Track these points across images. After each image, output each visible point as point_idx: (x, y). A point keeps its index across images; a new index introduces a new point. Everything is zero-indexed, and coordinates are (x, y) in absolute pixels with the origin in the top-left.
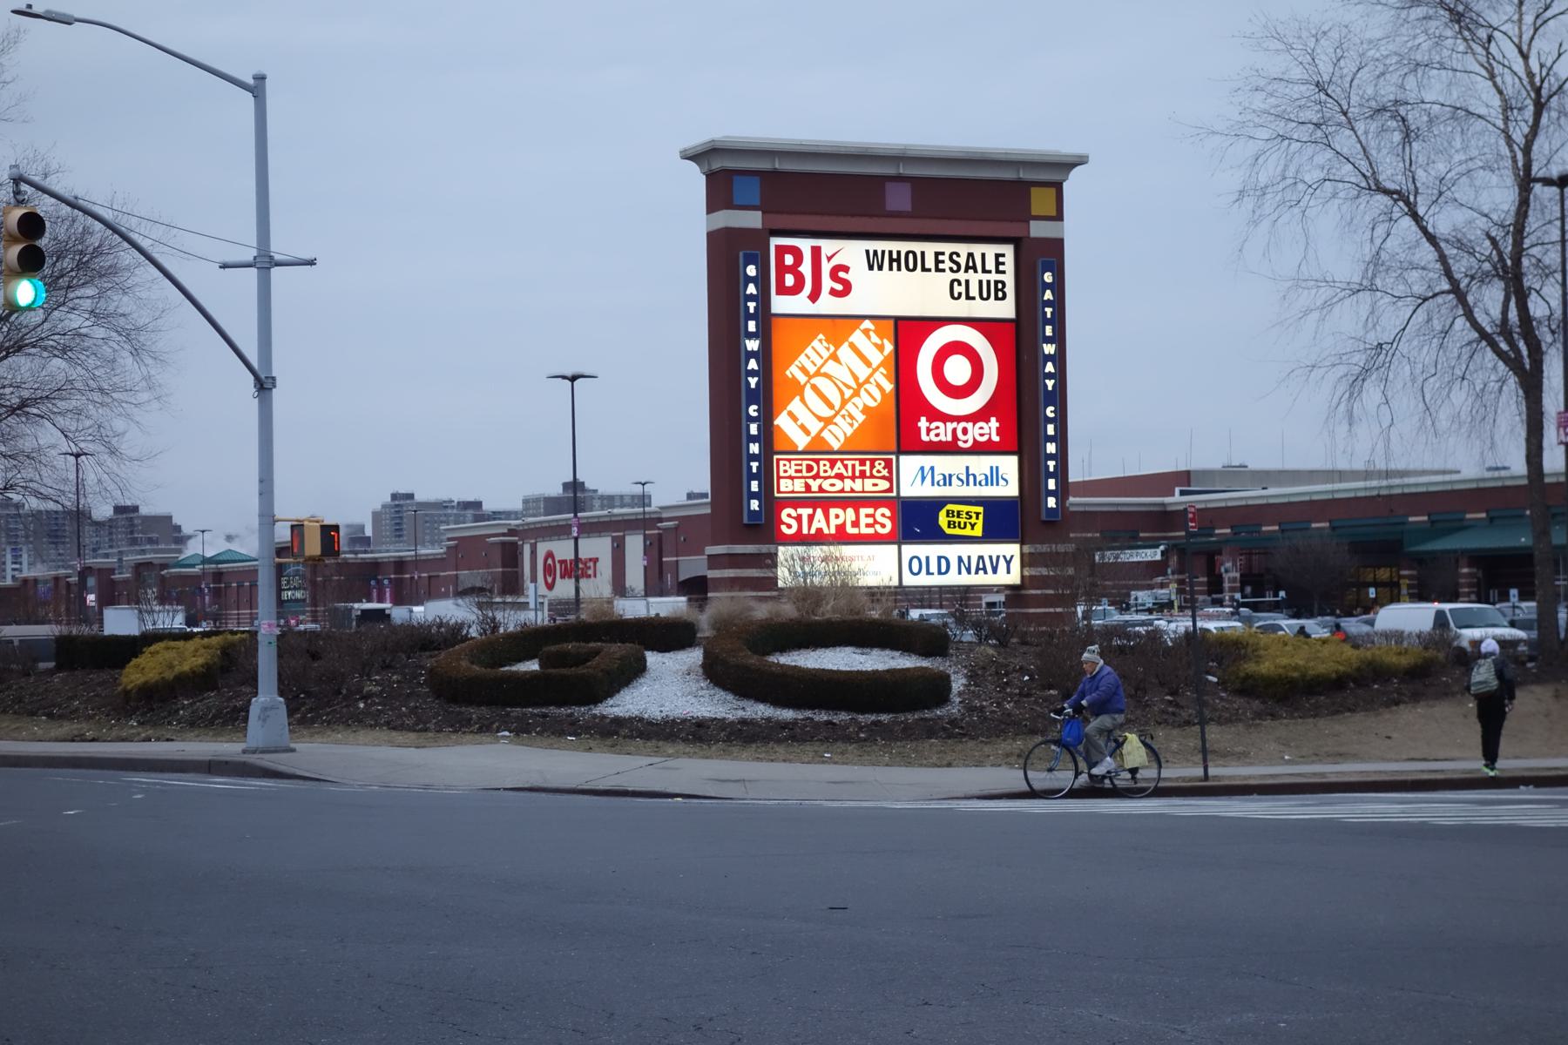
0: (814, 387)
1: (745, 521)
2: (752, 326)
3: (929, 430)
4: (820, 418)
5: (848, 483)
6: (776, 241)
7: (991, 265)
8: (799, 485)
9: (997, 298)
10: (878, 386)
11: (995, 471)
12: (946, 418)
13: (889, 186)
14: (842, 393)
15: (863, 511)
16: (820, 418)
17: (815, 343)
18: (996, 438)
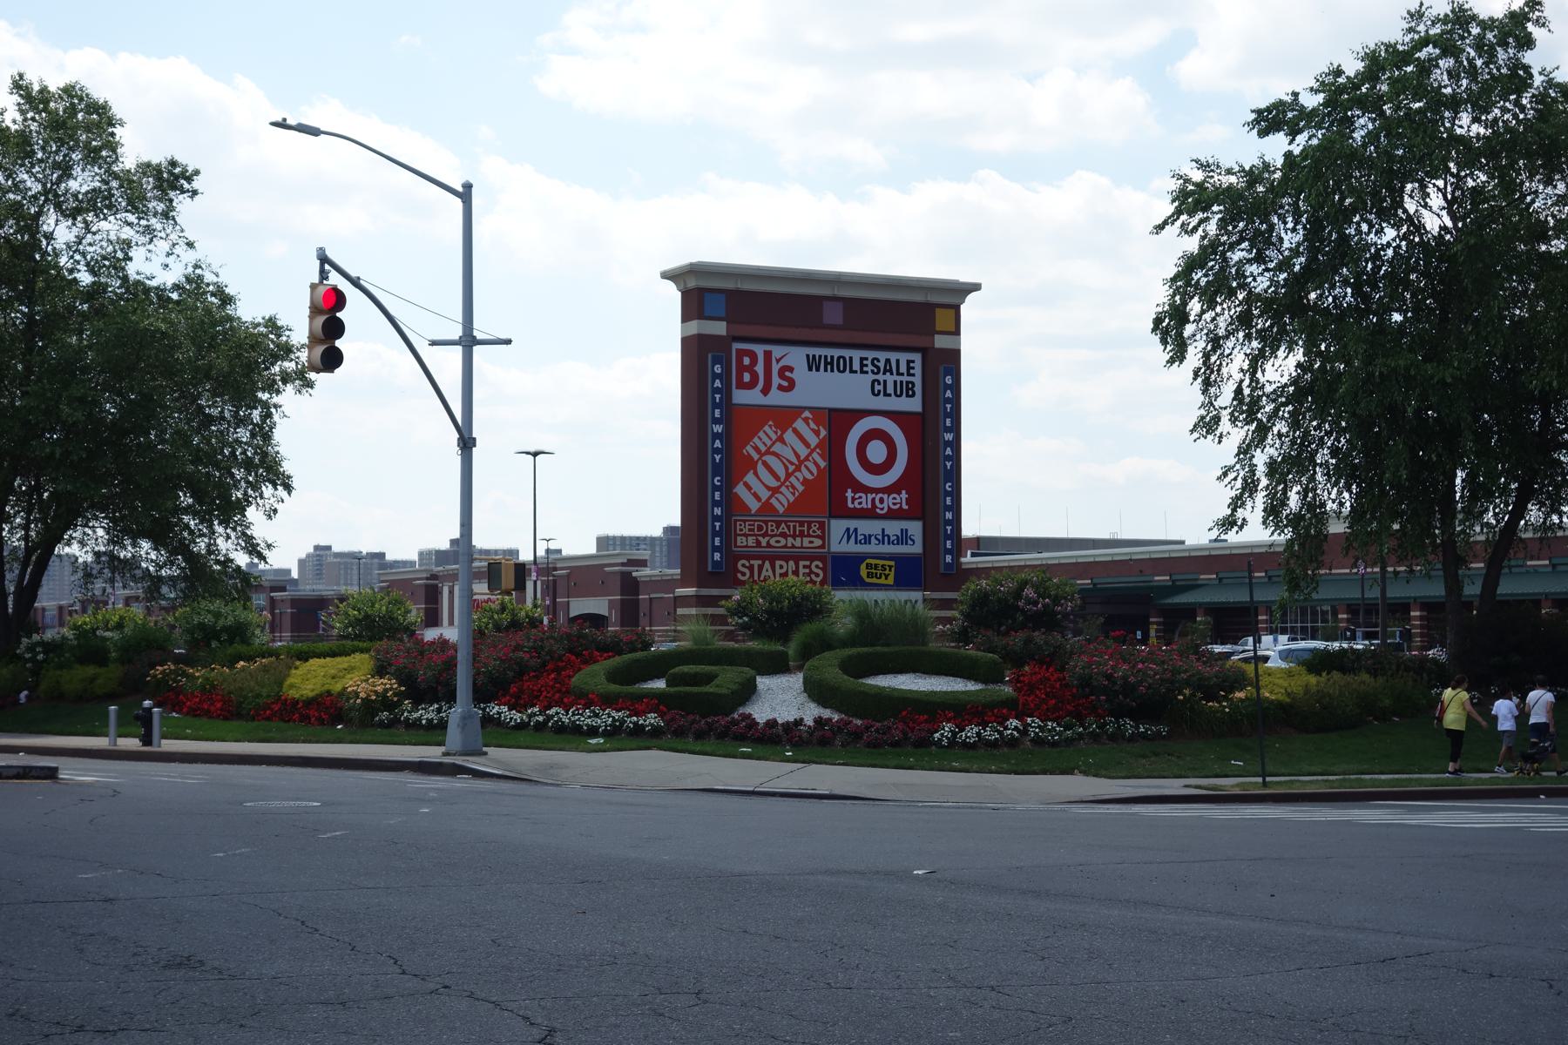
0: (765, 464)
2: (717, 413)
3: (853, 499)
5: (790, 540)
6: (737, 346)
7: (903, 369)
8: (751, 541)
10: (816, 464)
11: (904, 532)
12: (867, 490)
15: (802, 563)
17: (766, 428)
18: (905, 507)
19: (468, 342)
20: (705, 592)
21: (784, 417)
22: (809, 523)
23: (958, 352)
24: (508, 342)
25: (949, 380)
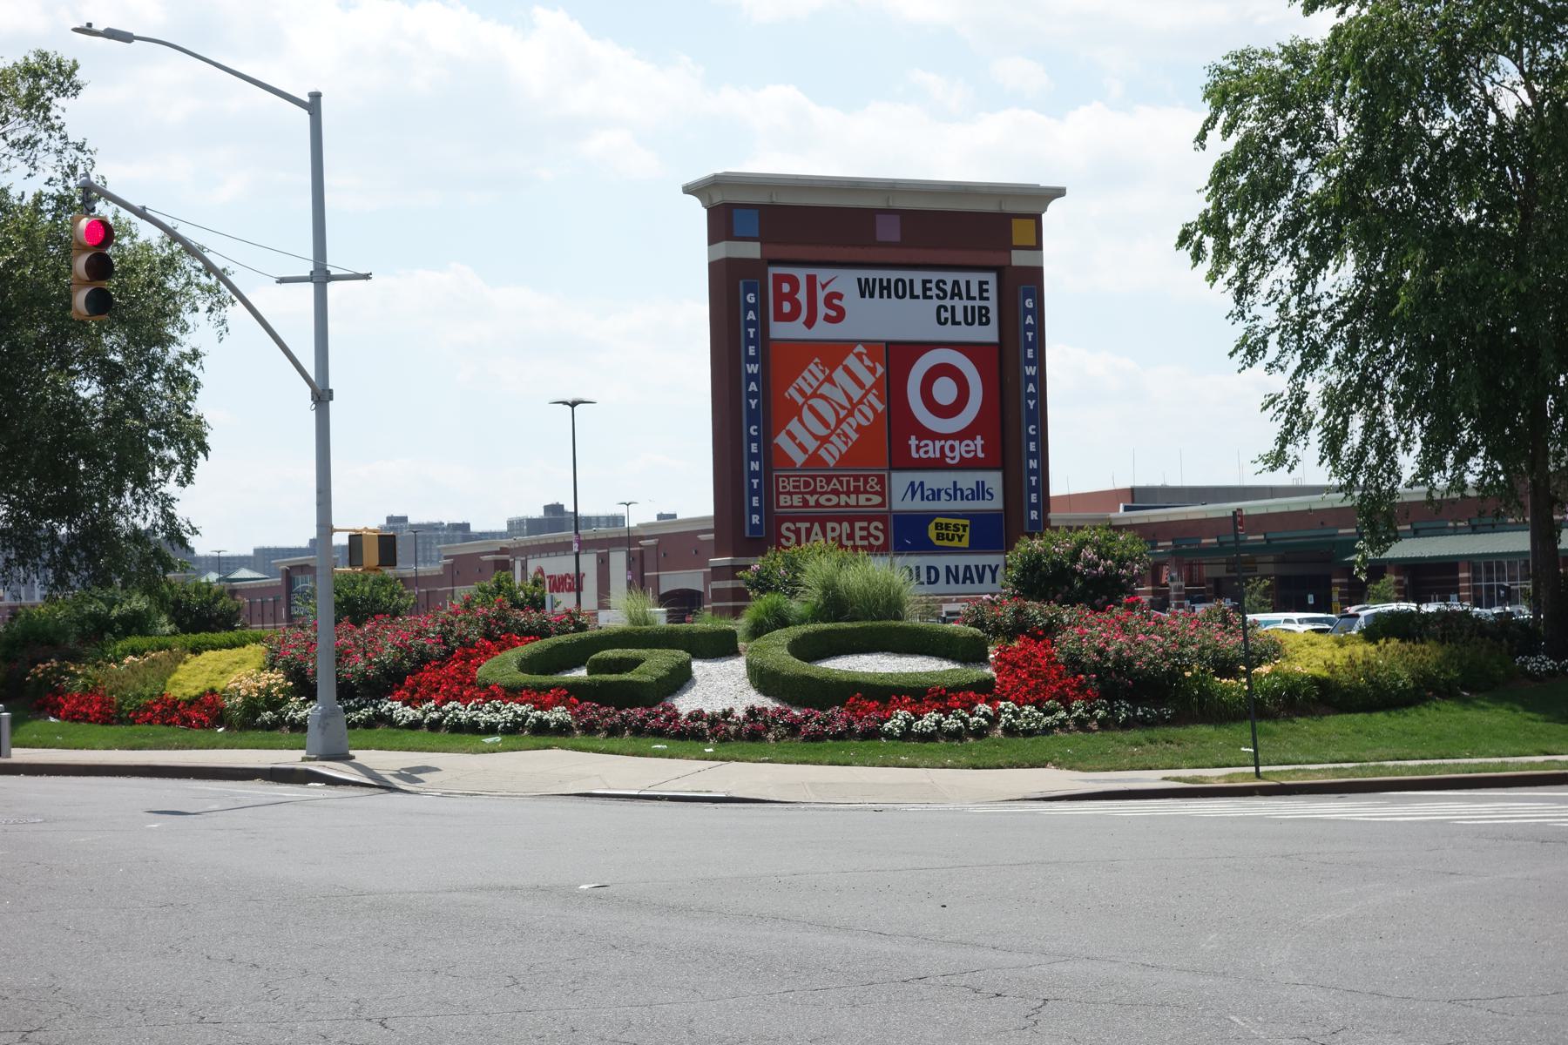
0: (812, 409)
1: (747, 534)
2: (752, 351)
3: (918, 448)
4: (816, 437)
5: (843, 498)
6: (773, 270)
7: (975, 292)
8: (797, 500)
9: (981, 323)
10: (871, 406)
11: (980, 485)
12: (935, 436)
13: (879, 217)
15: (858, 525)
16: (816, 437)
17: (812, 367)
18: (981, 455)
21: (833, 353)
23: (1041, 269)
25: (1029, 303)
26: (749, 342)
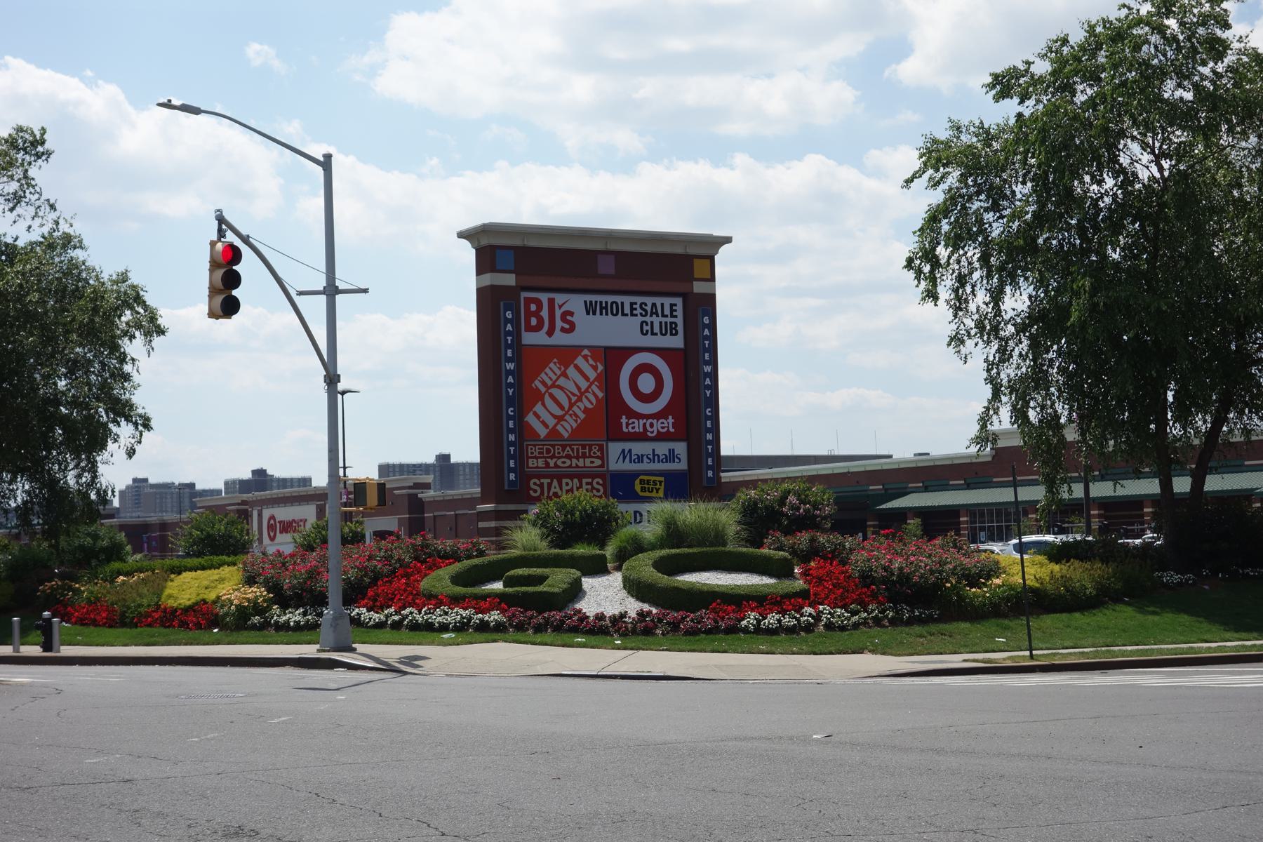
0: (551, 396)
2: (509, 353)
3: (628, 425)
4: (554, 416)
5: (574, 461)
6: (524, 295)
7: (667, 312)
8: (541, 463)
10: (594, 394)
11: (672, 451)
12: (639, 416)
14: (570, 399)
15: (584, 481)
16: (554, 416)
17: (552, 365)
18: (672, 430)
19: (331, 291)
20: (503, 507)
21: (567, 355)
22: (590, 446)
24: (365, 291)
25: (706, 320)
26: (508, 346)
